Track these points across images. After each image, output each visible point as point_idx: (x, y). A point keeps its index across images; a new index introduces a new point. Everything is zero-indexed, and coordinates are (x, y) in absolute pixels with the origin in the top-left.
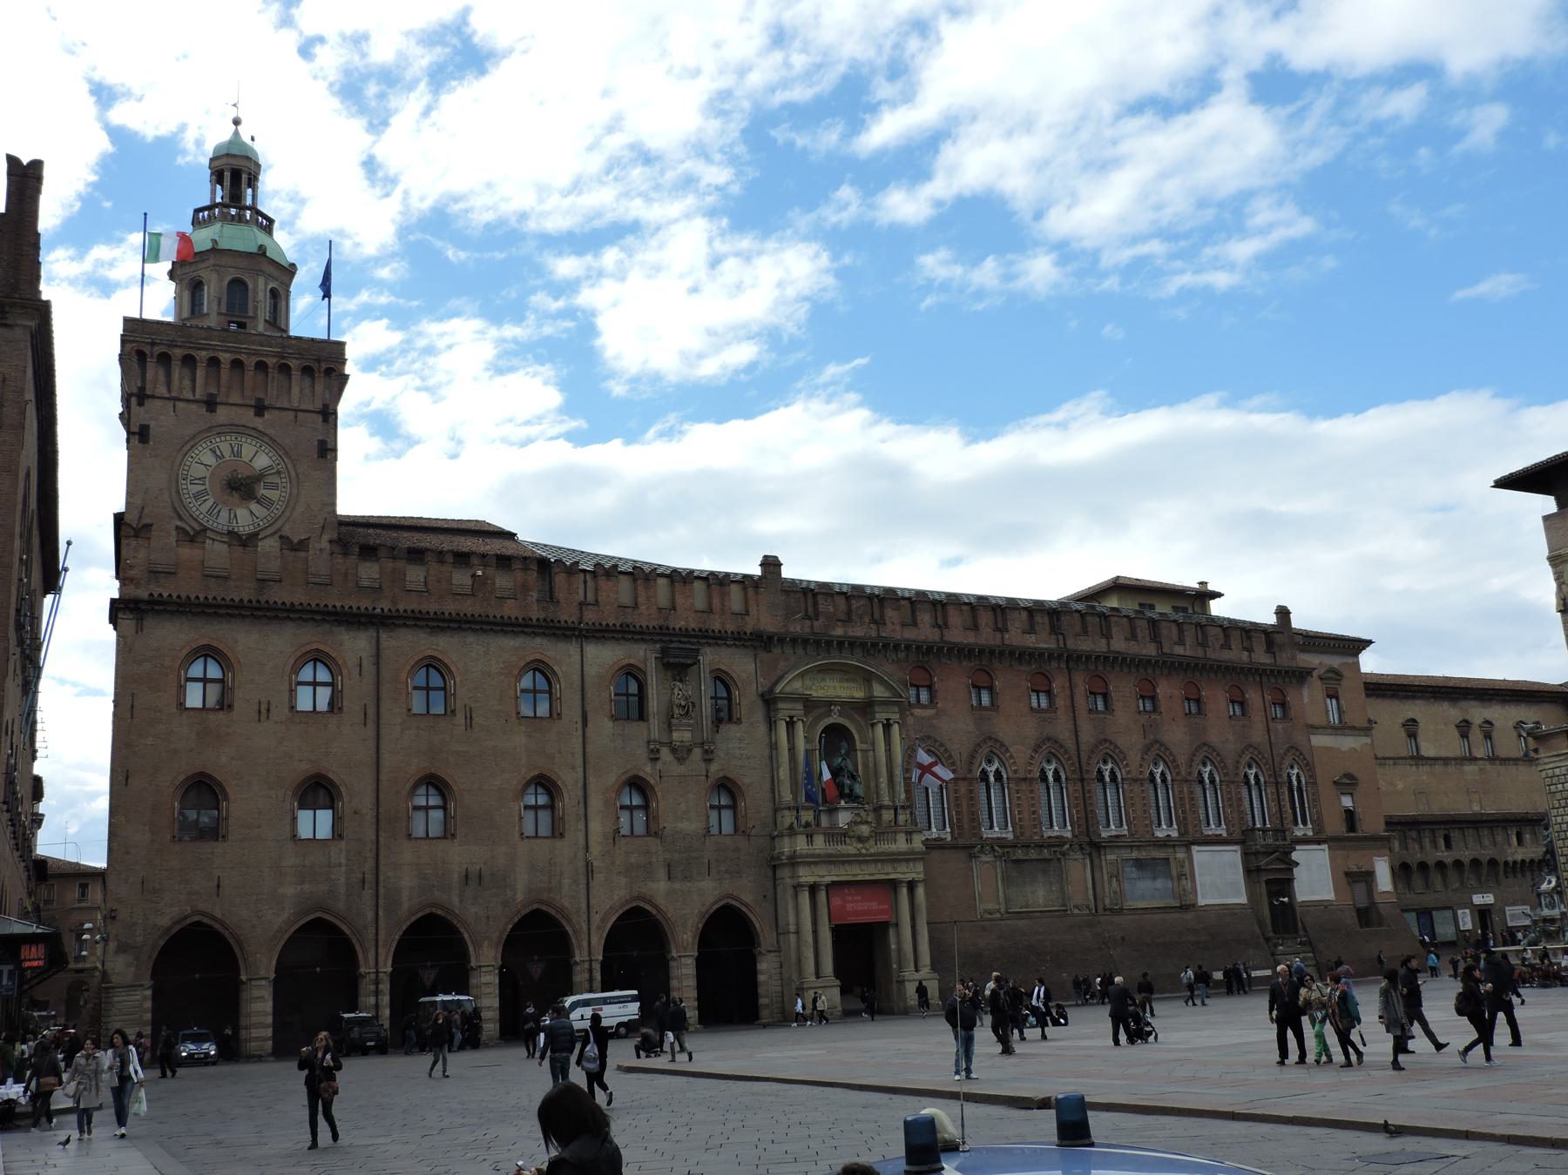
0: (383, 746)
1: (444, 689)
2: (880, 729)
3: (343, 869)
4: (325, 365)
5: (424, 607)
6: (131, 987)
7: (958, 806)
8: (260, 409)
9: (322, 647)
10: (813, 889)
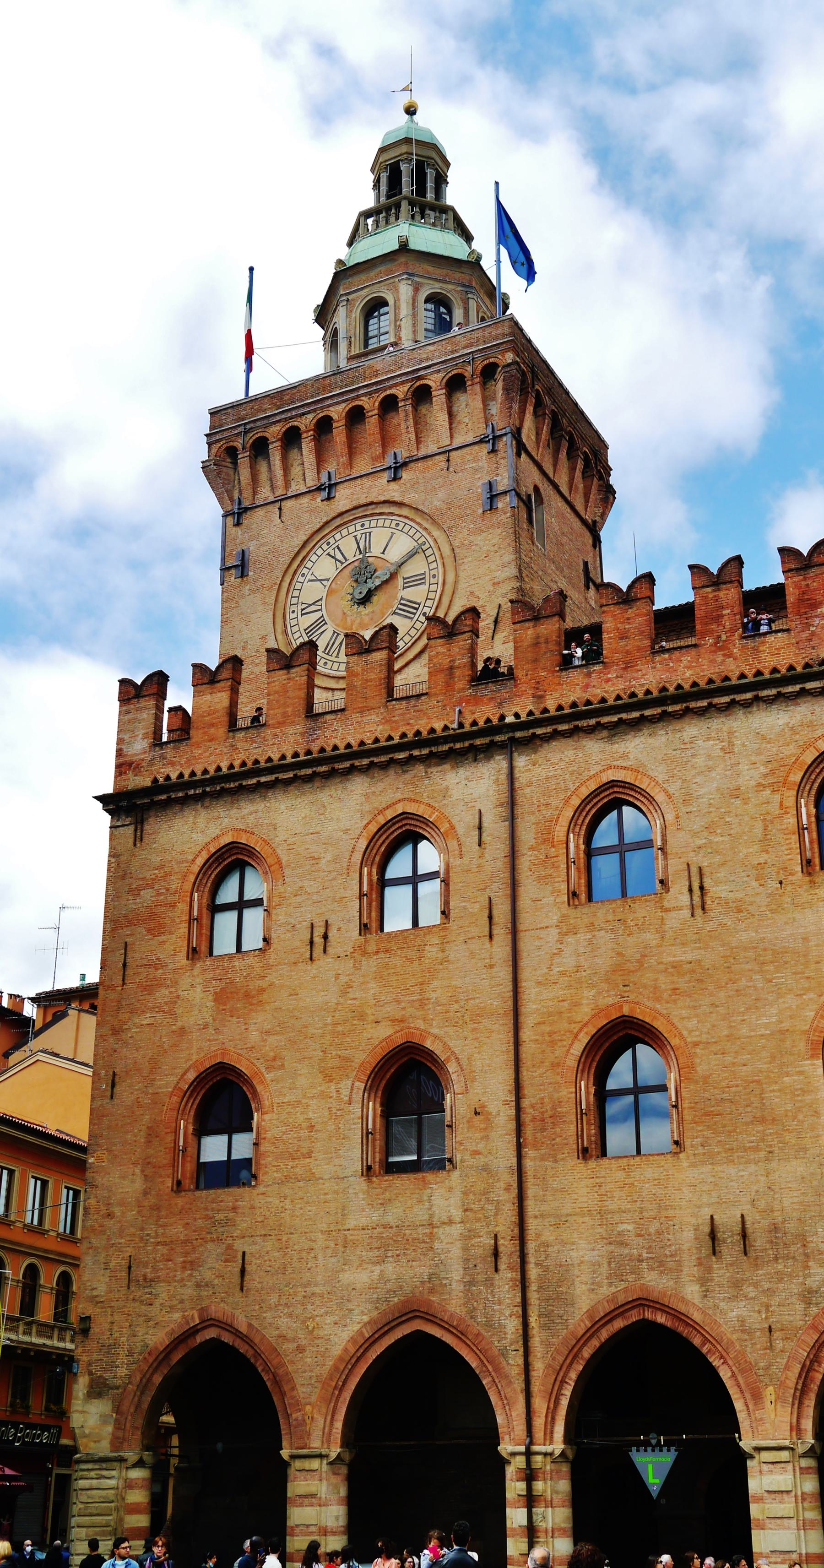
0: (526, 974)
3: (457, 1230)
5: (596, 692)
8: (397, 470)
9: (411, 808)
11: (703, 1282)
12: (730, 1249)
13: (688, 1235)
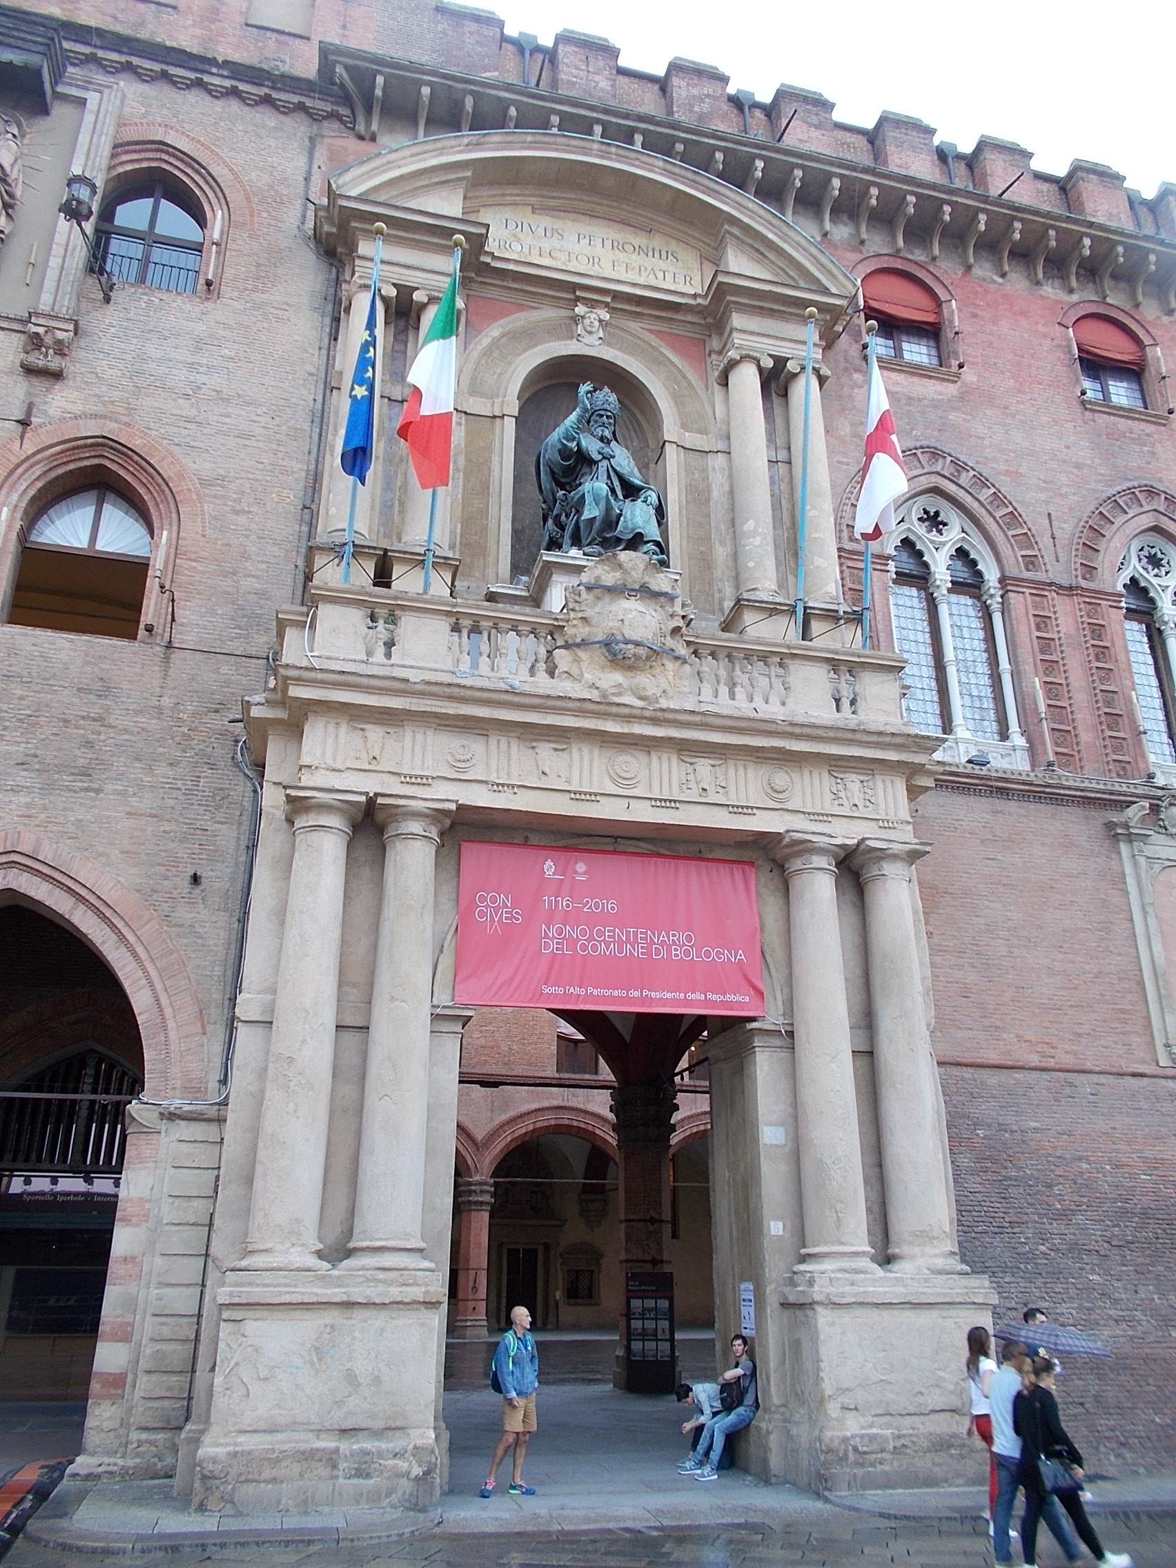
2: (747, 380)
7: (1050, 666)
10: (370, 824)
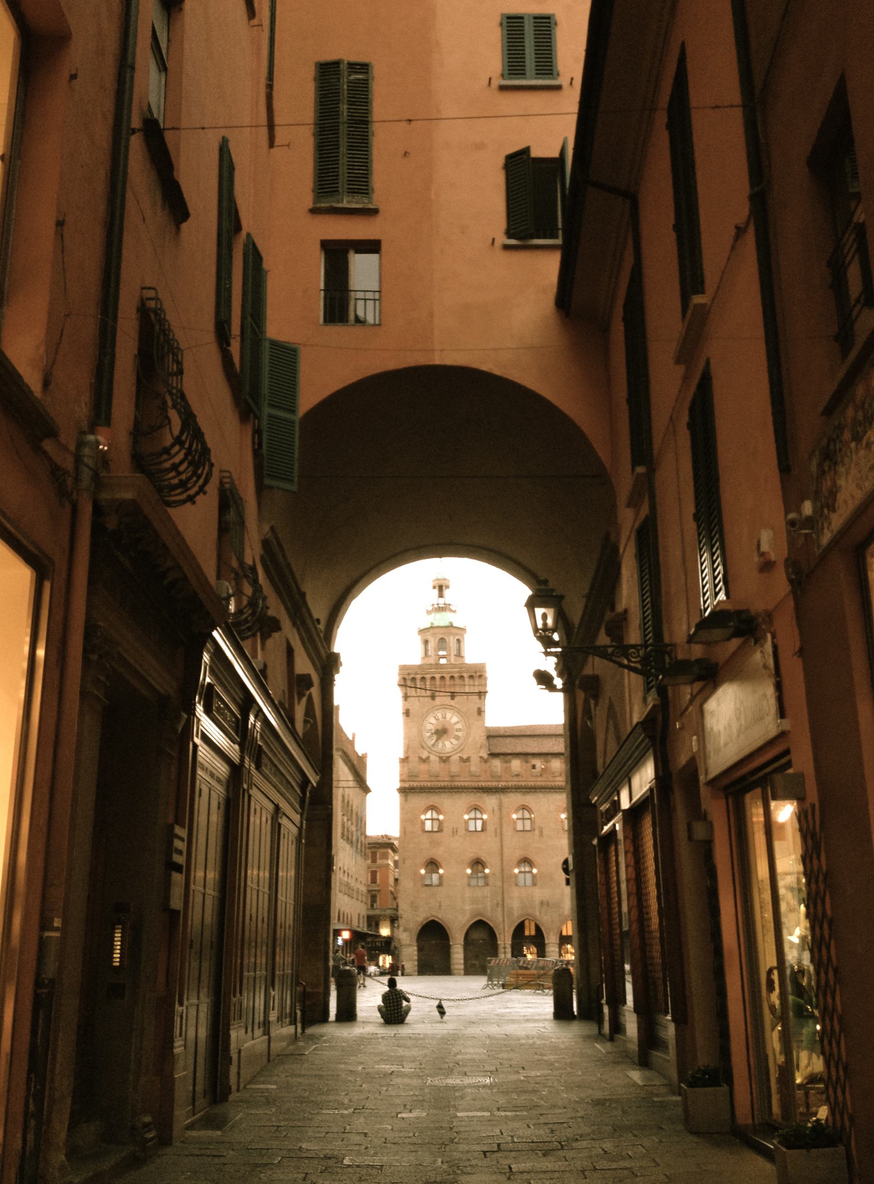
1: (530, 819)
4: (477, 674)
5: (520, 784)
6: (410, 945)
8: (453, 695)
11: (540, 913)
12: (545, 906)
13: (537, 903)
